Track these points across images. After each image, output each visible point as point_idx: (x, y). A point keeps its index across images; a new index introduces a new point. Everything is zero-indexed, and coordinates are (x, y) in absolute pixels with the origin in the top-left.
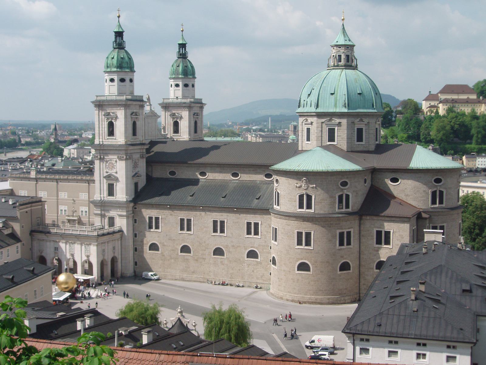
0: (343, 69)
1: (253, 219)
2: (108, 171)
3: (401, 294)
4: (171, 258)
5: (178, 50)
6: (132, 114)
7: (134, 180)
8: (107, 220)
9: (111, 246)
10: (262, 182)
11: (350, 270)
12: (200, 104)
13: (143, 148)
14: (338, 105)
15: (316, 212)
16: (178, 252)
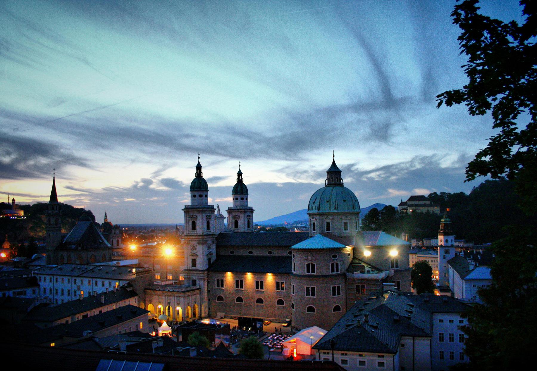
0: (334, 186)
2: (192, 251)
3: (354, 323)
4: (231, 305)
5: (237, 178)
6: (206, 217)
7: (208, 257)
8: (191, 281)
9: (193, 297)
11: (340, 310)
12: (251, 210)
13: (213, 237)
14: (331, 208)
15: (318, 274)
16: (235, 301)
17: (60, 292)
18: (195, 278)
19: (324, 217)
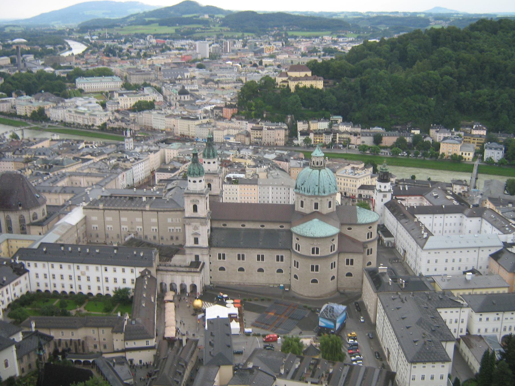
1: (280, 253)
10: (278, 230)
17: (58, 277)
18: (197, 254)
19: (313, 199)
